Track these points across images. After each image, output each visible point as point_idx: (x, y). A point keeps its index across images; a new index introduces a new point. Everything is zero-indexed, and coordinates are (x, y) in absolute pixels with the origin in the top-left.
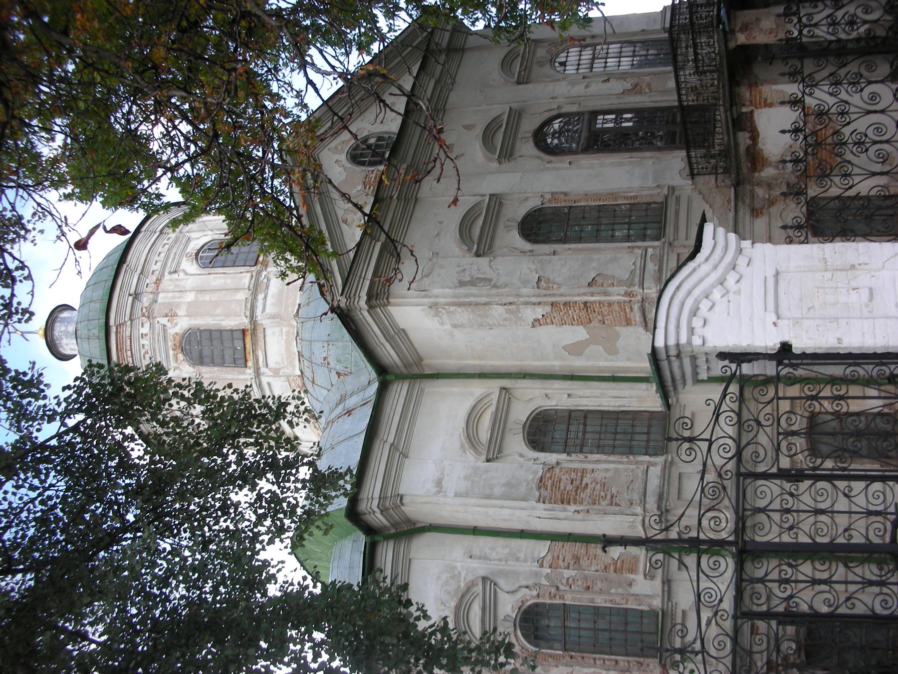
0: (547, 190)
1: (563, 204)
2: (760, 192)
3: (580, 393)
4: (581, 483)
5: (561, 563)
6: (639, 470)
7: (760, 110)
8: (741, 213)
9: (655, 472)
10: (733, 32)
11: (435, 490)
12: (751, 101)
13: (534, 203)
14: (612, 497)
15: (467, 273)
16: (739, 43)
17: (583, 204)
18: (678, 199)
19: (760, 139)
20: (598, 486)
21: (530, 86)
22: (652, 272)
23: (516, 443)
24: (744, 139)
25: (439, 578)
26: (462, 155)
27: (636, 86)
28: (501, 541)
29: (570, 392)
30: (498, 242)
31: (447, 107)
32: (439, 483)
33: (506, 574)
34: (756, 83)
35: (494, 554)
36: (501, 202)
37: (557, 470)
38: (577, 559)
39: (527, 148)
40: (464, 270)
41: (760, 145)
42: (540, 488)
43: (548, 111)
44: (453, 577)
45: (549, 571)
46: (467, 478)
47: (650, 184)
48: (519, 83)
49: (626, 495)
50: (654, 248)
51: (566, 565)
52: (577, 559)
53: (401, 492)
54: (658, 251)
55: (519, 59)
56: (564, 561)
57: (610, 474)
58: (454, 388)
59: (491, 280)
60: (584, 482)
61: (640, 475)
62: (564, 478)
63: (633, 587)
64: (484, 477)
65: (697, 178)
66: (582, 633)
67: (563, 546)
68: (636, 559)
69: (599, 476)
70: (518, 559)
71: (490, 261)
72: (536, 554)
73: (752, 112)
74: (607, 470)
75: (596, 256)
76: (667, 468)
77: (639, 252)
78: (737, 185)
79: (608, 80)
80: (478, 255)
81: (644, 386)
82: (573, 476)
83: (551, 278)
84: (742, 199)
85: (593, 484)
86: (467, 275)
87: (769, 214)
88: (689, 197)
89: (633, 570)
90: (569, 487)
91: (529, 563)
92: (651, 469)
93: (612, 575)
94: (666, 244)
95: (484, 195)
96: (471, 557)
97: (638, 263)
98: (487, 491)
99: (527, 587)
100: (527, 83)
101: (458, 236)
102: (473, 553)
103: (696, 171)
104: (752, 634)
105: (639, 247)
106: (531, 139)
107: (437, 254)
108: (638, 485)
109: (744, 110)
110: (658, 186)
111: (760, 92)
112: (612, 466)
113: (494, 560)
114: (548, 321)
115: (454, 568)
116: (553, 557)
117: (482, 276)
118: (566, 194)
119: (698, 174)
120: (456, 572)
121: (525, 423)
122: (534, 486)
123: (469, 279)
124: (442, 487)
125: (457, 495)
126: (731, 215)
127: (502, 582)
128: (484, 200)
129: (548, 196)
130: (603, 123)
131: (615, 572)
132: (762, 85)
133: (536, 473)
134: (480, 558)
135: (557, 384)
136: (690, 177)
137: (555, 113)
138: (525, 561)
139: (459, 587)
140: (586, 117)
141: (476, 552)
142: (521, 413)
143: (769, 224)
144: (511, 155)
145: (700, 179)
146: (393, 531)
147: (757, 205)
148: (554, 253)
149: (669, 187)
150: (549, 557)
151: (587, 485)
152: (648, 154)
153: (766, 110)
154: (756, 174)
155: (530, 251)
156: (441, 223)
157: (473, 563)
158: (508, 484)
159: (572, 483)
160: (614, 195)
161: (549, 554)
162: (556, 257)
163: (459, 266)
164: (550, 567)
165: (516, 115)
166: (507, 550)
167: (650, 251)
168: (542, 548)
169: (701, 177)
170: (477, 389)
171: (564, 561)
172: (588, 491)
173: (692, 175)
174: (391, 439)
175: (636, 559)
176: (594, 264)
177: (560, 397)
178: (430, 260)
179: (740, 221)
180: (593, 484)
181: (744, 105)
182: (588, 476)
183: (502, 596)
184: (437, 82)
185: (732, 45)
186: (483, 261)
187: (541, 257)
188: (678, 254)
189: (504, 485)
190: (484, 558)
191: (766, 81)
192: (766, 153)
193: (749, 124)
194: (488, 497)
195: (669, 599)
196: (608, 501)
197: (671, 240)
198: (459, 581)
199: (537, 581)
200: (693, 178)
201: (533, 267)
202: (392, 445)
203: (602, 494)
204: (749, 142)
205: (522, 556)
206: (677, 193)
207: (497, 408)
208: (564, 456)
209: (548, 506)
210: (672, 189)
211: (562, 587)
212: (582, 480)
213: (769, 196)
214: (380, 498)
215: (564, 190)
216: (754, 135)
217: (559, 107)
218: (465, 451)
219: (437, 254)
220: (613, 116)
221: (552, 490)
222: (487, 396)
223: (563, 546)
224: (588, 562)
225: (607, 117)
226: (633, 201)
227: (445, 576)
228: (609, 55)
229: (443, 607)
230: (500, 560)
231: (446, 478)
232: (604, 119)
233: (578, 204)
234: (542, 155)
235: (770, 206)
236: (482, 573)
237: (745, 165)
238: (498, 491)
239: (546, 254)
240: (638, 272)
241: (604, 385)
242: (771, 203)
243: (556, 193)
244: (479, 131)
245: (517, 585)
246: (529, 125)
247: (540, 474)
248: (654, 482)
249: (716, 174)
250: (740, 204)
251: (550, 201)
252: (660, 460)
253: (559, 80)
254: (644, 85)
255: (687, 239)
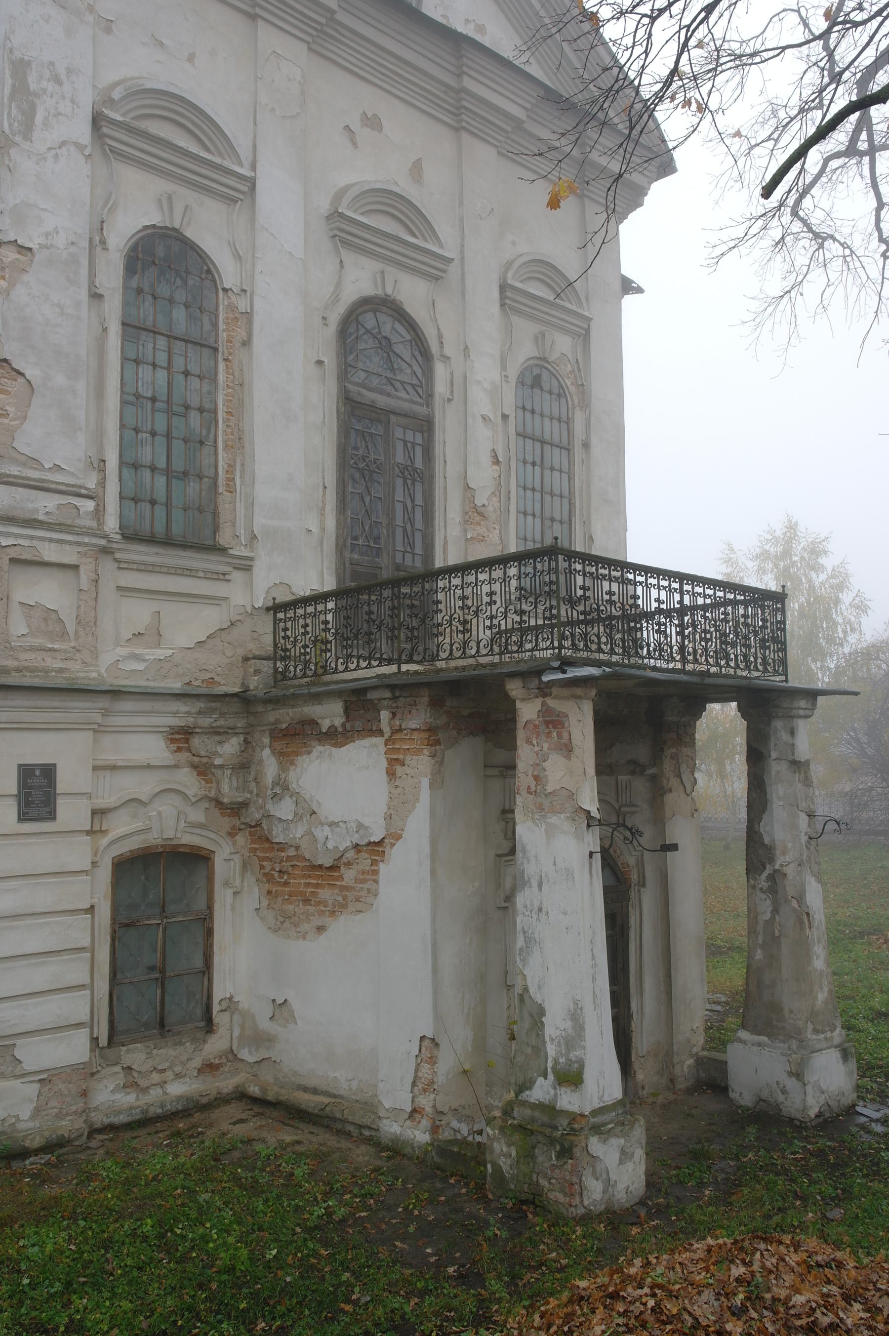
0: (258, 304)
1: (223, 335)
2: (231, 747)
7: (383, 749)
8: (182, 707)
10: (544, 690)
12: (400, 730)
13: (229, 273)
15: (50, 87)
16: (519, 705)
17: (221, 377)
18: (223, 577)
19: (327, 749)
21: (496, 309)
22: (30, 506)
24: (330, 713)
26: (355, 144)
27: (481, 514)
30: (129, 175)
31: (465, 135)
34: (438, 742)
36: (234, 201)
39: (361, 279)
40: (58, 81)
41: (318, 749)
43: (440, 336)
47: (260, 522)
48: (504, 287)
50: (99, 513)
54: (89, 523)
55: (551, 297)
59: (27, 137)
65: (270, 617)
71: (80, 147)
73: (380, 733)
75: (81, 386)
77: (91, 482)
78: (244, 700)
79: (497, 462)
80: (97, 120)
83: (25, 277)
84: (214, 710)
86: (44, 84)
87: (176, 766)
88: (226, 599)
94: (103, 542)
95: (253, 167)
97: (58, 477)
100: (502, 305)
101: (149, 85)
103: (281, 615)
105: (102, 483)
106: (380, 292)
107: (108, 30)
109: (385, 715)
110: (254, 537)
111: (419, 751)
117: (39, 119)
118: (247, 343)
119: (276, 621)
123: (33, 86)
126: (176, 685)
128: (240, 164)
129: (242, 305)
130: (405, 443)
132: (433, 756)
136: (270, 604)
137: (434, 348)
140: (422, 410)
143: (149, 767)
144: (345, 243)
145: (265, 625)
147: (196, 741)
148: (96, 296)
149: (251, 559)
152: (331, 523)
153: (385, 764)
154: (266, 740)
155: (103, 242)
156: (191, 58)
160: (239, 443)
162: (83, 295)
163: (69, 71)
165: (434, 269)
167: (89, 505)
169: (270, 628)
173: (276, 608)
176: (60, 380)
178: (91, 9)
179: (158, 705)
181: (394, 714)
184: (518, 123)
185: (514, 688)
186: (82, 131)
187: (85, 262)
188: (76, 567)
191: (441, 763)
192: (303, 761)
193: (358, 725)
197: (118, 555)
200: (268, 609)
201: (60, 241)
204: (325, 725)
206: (237, 576)
210: (246, 566)
213: (221, 767)
215: (255, 340)
216: (336, 737)
217: (446, 359)
219: (108, 30)
220: (419, 463)
225: (419, 451)
226: (221, 481)
228: (547, 472)
232: (414, 445)
233: (221, 366)
234: (341, 309)
235: (194, 767)
237: (286, 715)
239: (92, 274)
240: (35, 475)
242: (203, 770)
243: (250, 323)
244: (406, 187)
246: (411, 293)
249: (274, 658)
250: (201, 705)
251: (232, 308)
253: (504, 367)
254: (481, 530)
255: (119, 588)
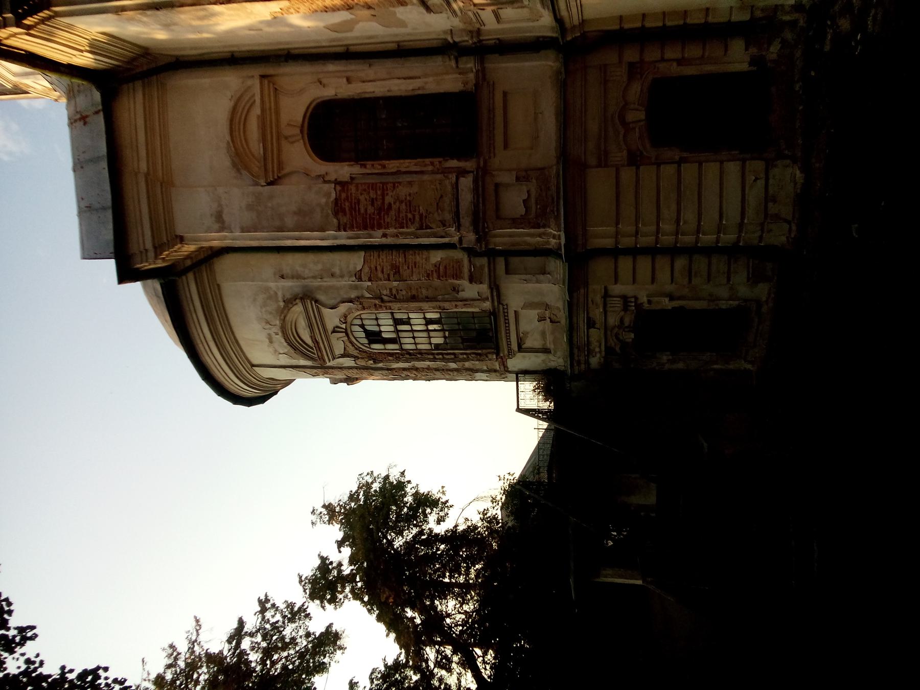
3: (362, 75)
4: (383, 203)
5: (380, 275)
6: (447, 182)
9: (466, 183)
11: (216, 226)
14: (421, 216)
20: (403, 206)
23: (298, 155)
25: (255, 300)
28: (310, 257)
29: (349, 74)
32: (219, 217)
33: (326, 290)
35: (307, 271)
37: (353, 188)
38: (396, 269)
42: (336, 214)
44: (270, 298)
45: (369, 284)
46: (250, 207)
49: (436, 214)
51: (386, 276)
52: (396, 269)
53: (179, 233)
56: (383, 272)
57: (415, 189)
58: (204, 80)
60: (386, 202)
61: (449, 188)
62: (362, 198)
63: (460, 293)
64: (270, 205)
66: (416, 334)
67: (379, 256)
68: (459, 262)
69: (403, 191)
70: (333, 275)
72: (351, 267)
74: (410, 183)
76: (482, 175)
81: (439, 60)
82: (373, 195)
85: (398, 204)
89: (458, 276)
90: (371, 210)
91: (346, 279)
92: (462, 180)
93: (437, 282)
96: (282, 277)
98: (277, 223)
99: (351, 301)
102: (284, 272)
104: (589, 328)
108: (447, 200)
112: (415, 178)
113: (308, 278)
114: (292, 10)
115: (267, 289)
116: (370, 268)
120: (272, 293)
121: (302, 126)
122: (330, 212)
124: (223, 222)
125: (243, 230)
127: (322, 297)
131: (439, 278)
133: (328, 195)
134: (293, 277)
135: (331, 67)
138: (342, 276)
139: (279, 306)
141: (287, 270)
142: (294, 110)
146: (189, 263)
150: (366, 269)
151: (390, 204)
157: (288, 283)
158: (299, 212)
159: (373, 205)
161: (366, 266)
164: (370, 280)
166: (320, 267)
168: (357, 261)
170: (232, 81)
171: (383, 272)
172: (393, 213)
174: (143, 166)
175: (459, 262)
177: (336, 84)
180: (398, 204)
182: (390, 194)
183: (326, 312)
189: (295, 213)
190: (297, 277)
194: (281, 229)
195: (499, 302)
196: (417, 225)
198: (277, 301)
199: (360, 294)
202: (147, 175)
203: (410, 216)
205: (337, 270)
207: (263, 110)
208: (356, 169)
209: (350, 233)
211: (385, 298)
212: (383, 199)
214: (155, 248)
218: (238, 170)
221: (351, 214)
222: (246, 91)
223: (379, 256)
224: (408, 271)
227: (261, 298)
229: (268, 326)
230: (314, 277)
231: (225, 211)
236: (297, 290)
238: (290, 221)
241: (389, 64)
245: (339, 300)
247: (333, 195)
248: (466, 198)
252: (469, 165)
